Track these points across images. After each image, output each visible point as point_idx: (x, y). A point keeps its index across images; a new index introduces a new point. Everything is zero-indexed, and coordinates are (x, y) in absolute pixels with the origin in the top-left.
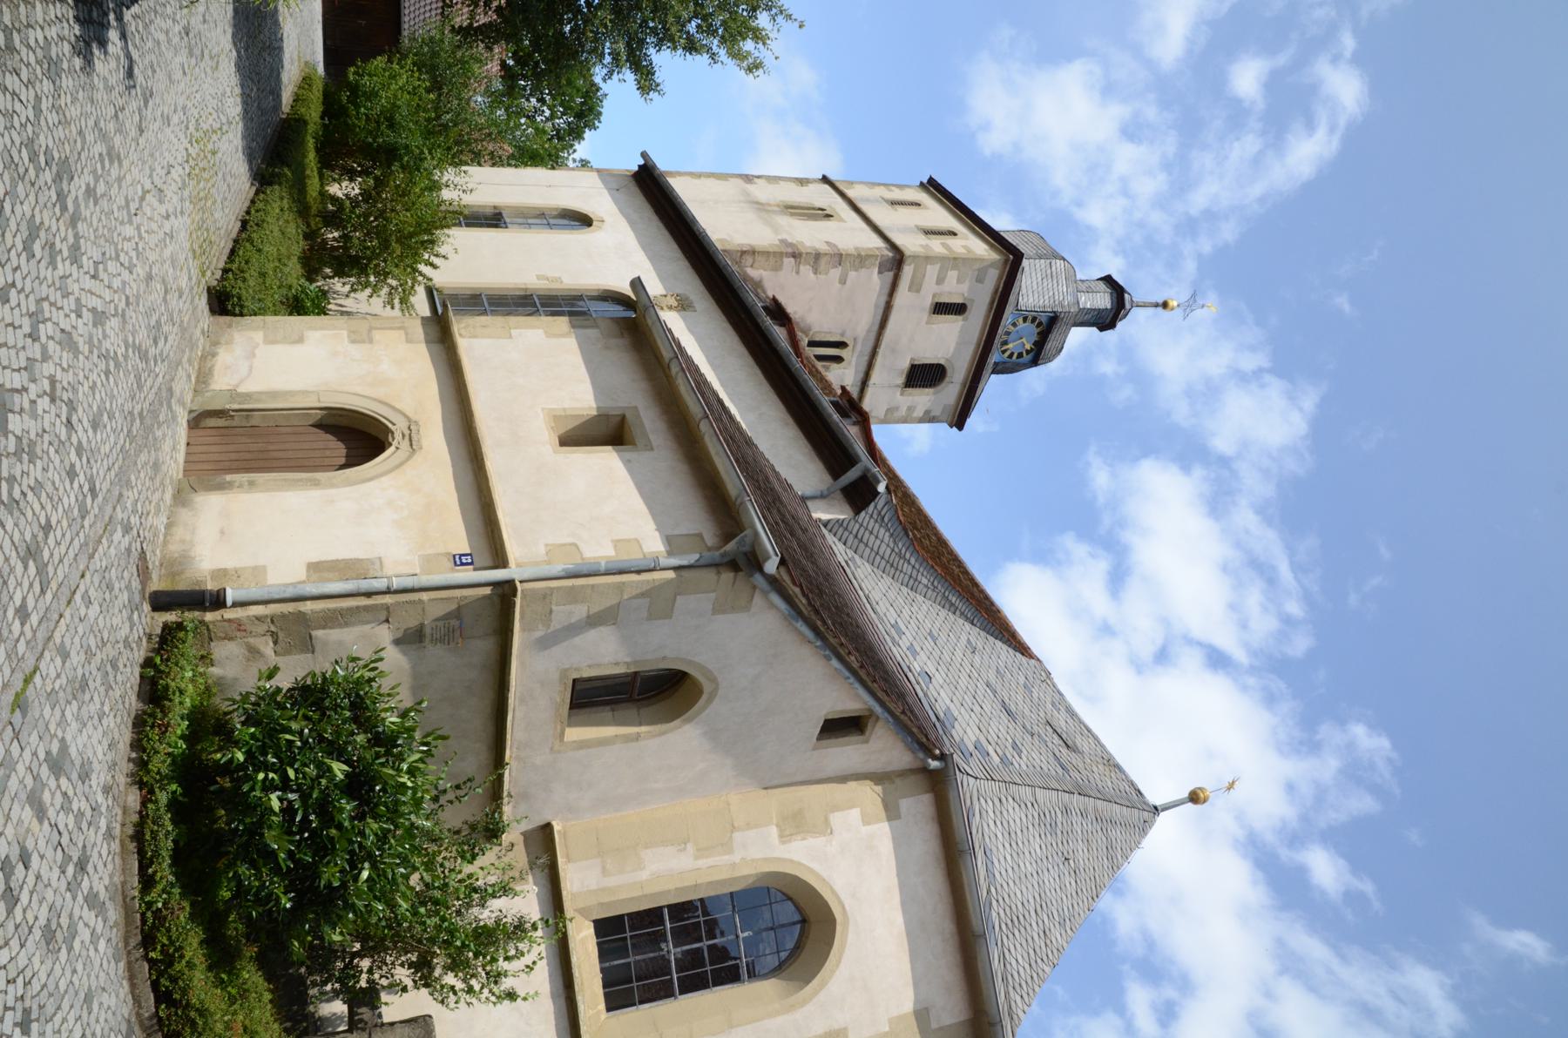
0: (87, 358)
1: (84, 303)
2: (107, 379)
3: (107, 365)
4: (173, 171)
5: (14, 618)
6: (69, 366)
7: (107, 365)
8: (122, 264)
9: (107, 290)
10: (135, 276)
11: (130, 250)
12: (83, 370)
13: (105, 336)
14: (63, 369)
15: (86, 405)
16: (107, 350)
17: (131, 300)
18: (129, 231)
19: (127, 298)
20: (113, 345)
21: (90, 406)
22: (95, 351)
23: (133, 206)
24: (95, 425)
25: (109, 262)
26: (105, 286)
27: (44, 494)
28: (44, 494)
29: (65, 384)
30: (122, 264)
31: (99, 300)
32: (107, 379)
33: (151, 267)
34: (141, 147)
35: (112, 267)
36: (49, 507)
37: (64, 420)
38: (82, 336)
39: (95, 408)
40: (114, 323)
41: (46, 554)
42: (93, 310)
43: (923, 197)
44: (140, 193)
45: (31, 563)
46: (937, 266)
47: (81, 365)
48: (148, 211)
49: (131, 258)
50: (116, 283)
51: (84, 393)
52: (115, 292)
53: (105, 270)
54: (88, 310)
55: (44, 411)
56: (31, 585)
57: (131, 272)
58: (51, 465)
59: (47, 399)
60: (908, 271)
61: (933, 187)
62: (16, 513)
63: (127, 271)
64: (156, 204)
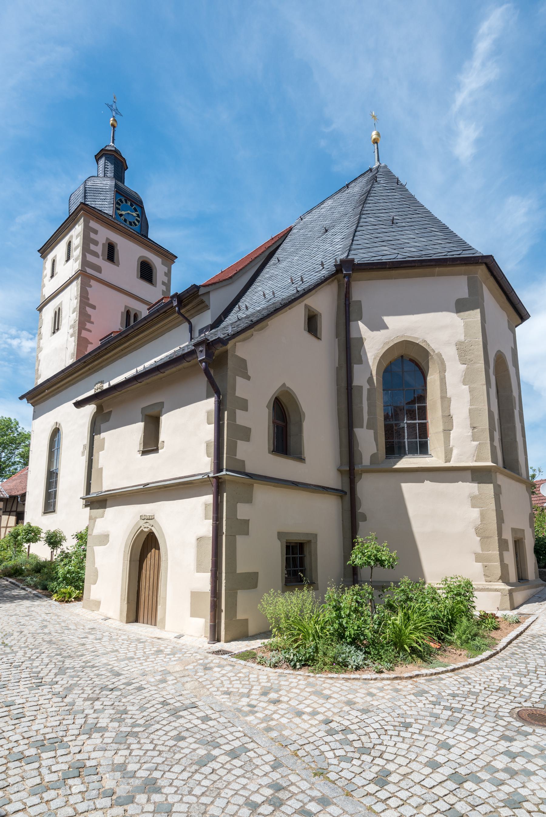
3: (89, 667)
5: (207, 724)
6: (82, 689)
10: (46, 650)
12: (87, 681)
13: (74, 668)
14: (83, 693)
17: (58, 653)
19: (57, 655)
22: (79, 674)
26: (46, 668)
28: (146, 706)
29: (90, 692)
35: (36, 664)
36: (154, 702)
39: (109, 674)
40: (68, 663)
41: (178, 704)
43: (50, 257)
45: (181, 713)
46: (87, 255)
47: (83, 682)
50: (46, 661)
51: (99, 681)
52: (51, 661)
56: (192, 714)
58: (132, 701)
60: (89, 271)
61: (44, 251)
62: (152, 722)
63: (42, 655)
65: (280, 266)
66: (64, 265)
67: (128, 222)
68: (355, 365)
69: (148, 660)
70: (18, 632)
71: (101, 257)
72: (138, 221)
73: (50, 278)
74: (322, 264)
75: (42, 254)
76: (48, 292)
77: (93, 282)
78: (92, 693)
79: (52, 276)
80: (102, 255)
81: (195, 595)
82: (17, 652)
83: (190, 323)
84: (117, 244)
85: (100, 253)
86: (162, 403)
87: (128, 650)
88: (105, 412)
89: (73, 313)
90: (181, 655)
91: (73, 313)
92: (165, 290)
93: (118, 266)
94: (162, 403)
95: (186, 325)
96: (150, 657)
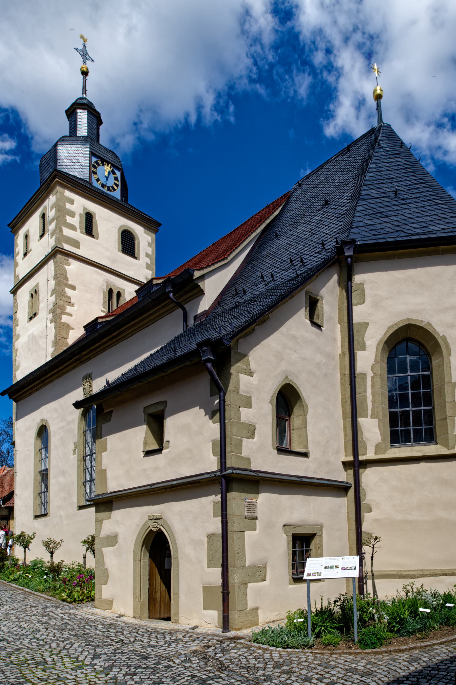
0: (115, 661)
1: (89, 663)
2: (125, 653)
3: (119, 653)
4: (23, 626)
6: (119, 668)
7: (119, 653)
8: (71, 647)
9: (83, 653)
11: (63, 644)
12: (121, 663)
15: (137, 662)
16: (111, 653)
18: (54, 645)
20: (108, 651)
21: (138, 660)
22: (112, 658)
23: (42, 643)
24: (146, 658)
25: (70, 652)
26: (81, 654)
27: (177, 678)
30: (71, 647)
31: (88, 657)
32: (125, 653)
33: (71, 635)
34: (12, 640)
35: (72, 651)
37: (144, 670)
38: (105, 664)
39: (139, 658)
40: (99, 651)
42: (93, 659)
43: (22, 232)
44: (35, 640)
47: (118, 664)
48: (44, 637)
49: (67, 644)
50: (80, 650)
51: (132, 662)
52: (84, 650)
53: (74, 654)
54: (93, 661)
55: (140, 678)
57: (74, 643)
59: (134, 677)
60: (67, 247)
64: (41, 633)
65: (278, 241)
66: (38, 241)
67: (106, 188)
68: (358, 352)
69: (170, 646)
70: (43, 628)
71: (79, 230)
72: (117, 185)
73: (23, 256)
74: (323, 244)
75: (13, 228)
76: (22, 271)
77: (71, 260)
78: (129, 671)
79: (25, 255)
80: (80, 227)
81: (207, 589)
82: (51, 644)
83: (184, 310)
84: (95, 214)
85: (77, 226)
86: (165, 402)
87: (150, 640)
88: (106, 411)
89: (51, 296)
90: (198, 642)
91: (51, 296)
92: (149, 262)
93: (98, 239)
94: (165, 402)
95: (179, 312)
96: (172, 644)
